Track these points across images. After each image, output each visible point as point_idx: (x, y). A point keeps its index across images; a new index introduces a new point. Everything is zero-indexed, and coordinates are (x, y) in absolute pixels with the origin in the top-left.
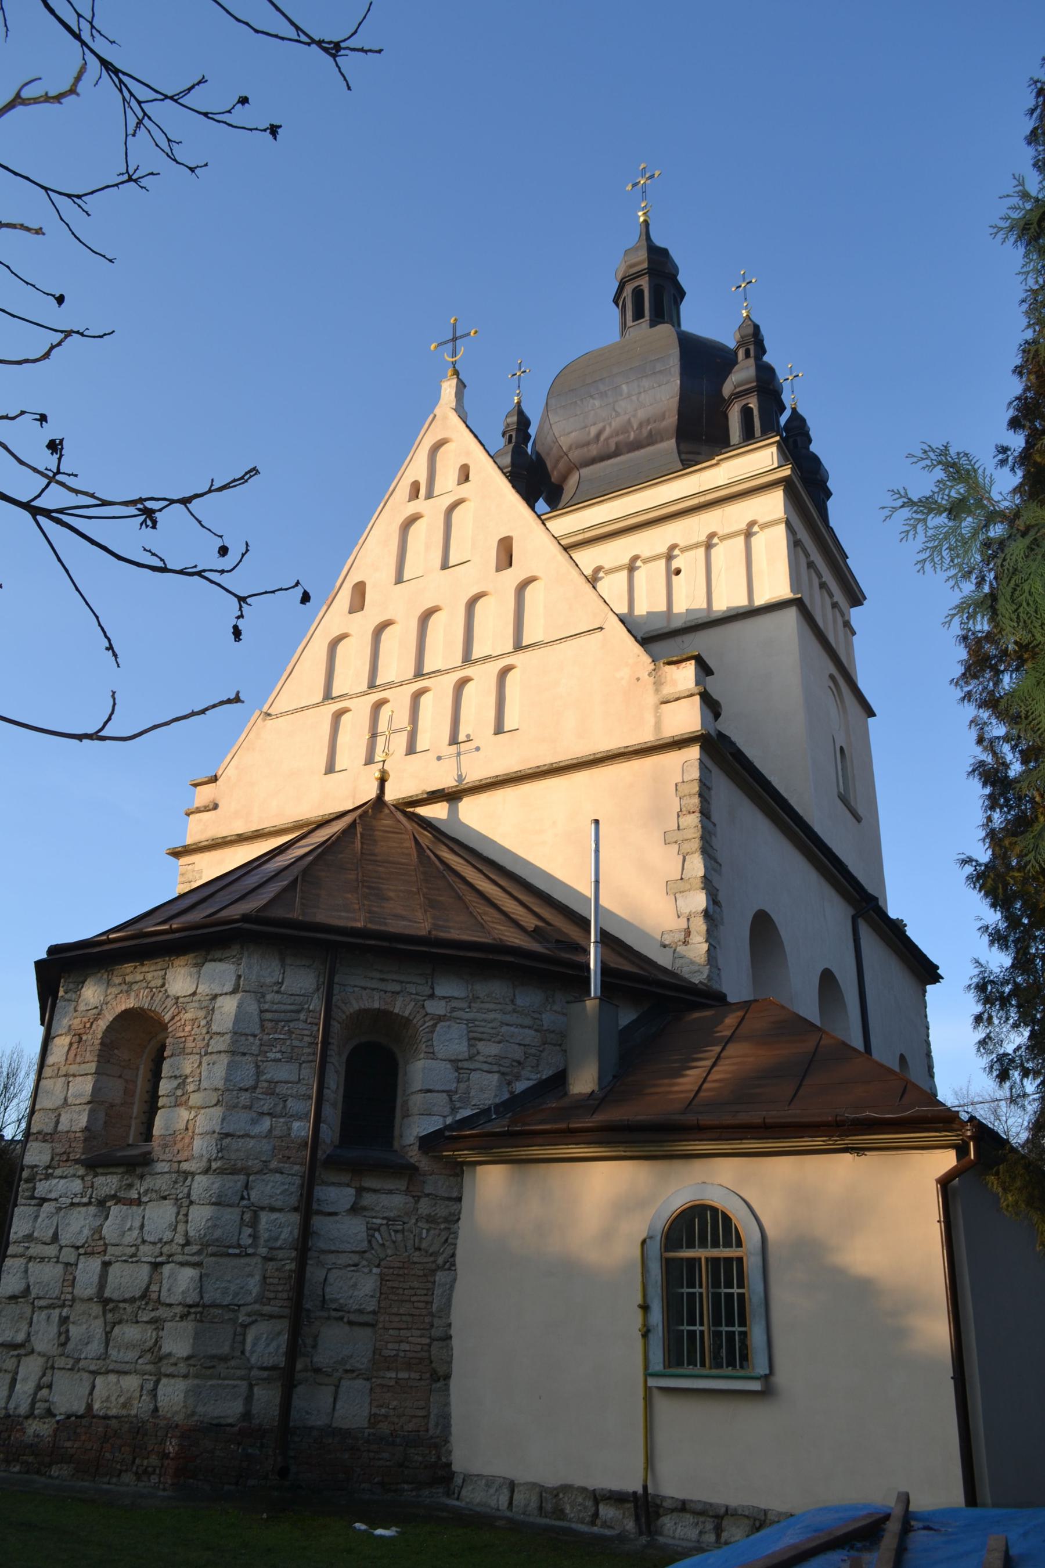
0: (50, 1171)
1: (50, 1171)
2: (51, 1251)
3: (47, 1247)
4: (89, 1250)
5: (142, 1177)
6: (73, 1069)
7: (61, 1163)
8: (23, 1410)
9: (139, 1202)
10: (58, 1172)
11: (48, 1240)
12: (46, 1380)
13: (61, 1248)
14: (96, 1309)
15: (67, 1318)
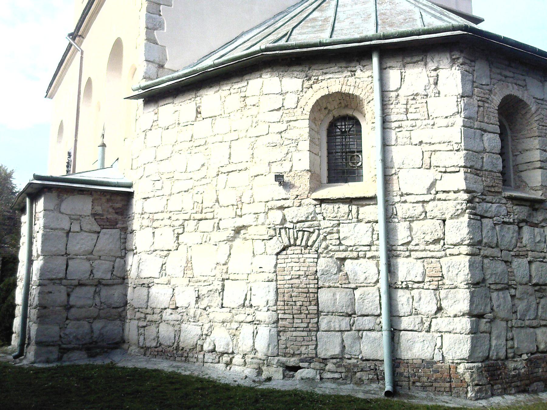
0: (484, 197)
1: (484, 197)
2: (496, 252)
3: (494, 250)
4: (517, 253)
5: (536, 210)
6: (484, 126)
7: (489, 193)
8: (502, 355)
9: (536, 225)
10: (489, 198)
11: (493, 246)
12: (510, 334)
13: (501, 251)
14: (531, 290)
15: (515, 296)
